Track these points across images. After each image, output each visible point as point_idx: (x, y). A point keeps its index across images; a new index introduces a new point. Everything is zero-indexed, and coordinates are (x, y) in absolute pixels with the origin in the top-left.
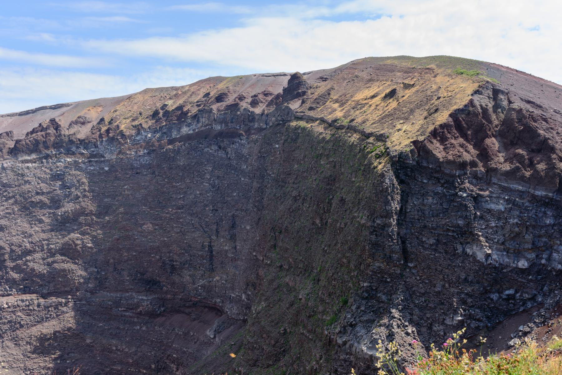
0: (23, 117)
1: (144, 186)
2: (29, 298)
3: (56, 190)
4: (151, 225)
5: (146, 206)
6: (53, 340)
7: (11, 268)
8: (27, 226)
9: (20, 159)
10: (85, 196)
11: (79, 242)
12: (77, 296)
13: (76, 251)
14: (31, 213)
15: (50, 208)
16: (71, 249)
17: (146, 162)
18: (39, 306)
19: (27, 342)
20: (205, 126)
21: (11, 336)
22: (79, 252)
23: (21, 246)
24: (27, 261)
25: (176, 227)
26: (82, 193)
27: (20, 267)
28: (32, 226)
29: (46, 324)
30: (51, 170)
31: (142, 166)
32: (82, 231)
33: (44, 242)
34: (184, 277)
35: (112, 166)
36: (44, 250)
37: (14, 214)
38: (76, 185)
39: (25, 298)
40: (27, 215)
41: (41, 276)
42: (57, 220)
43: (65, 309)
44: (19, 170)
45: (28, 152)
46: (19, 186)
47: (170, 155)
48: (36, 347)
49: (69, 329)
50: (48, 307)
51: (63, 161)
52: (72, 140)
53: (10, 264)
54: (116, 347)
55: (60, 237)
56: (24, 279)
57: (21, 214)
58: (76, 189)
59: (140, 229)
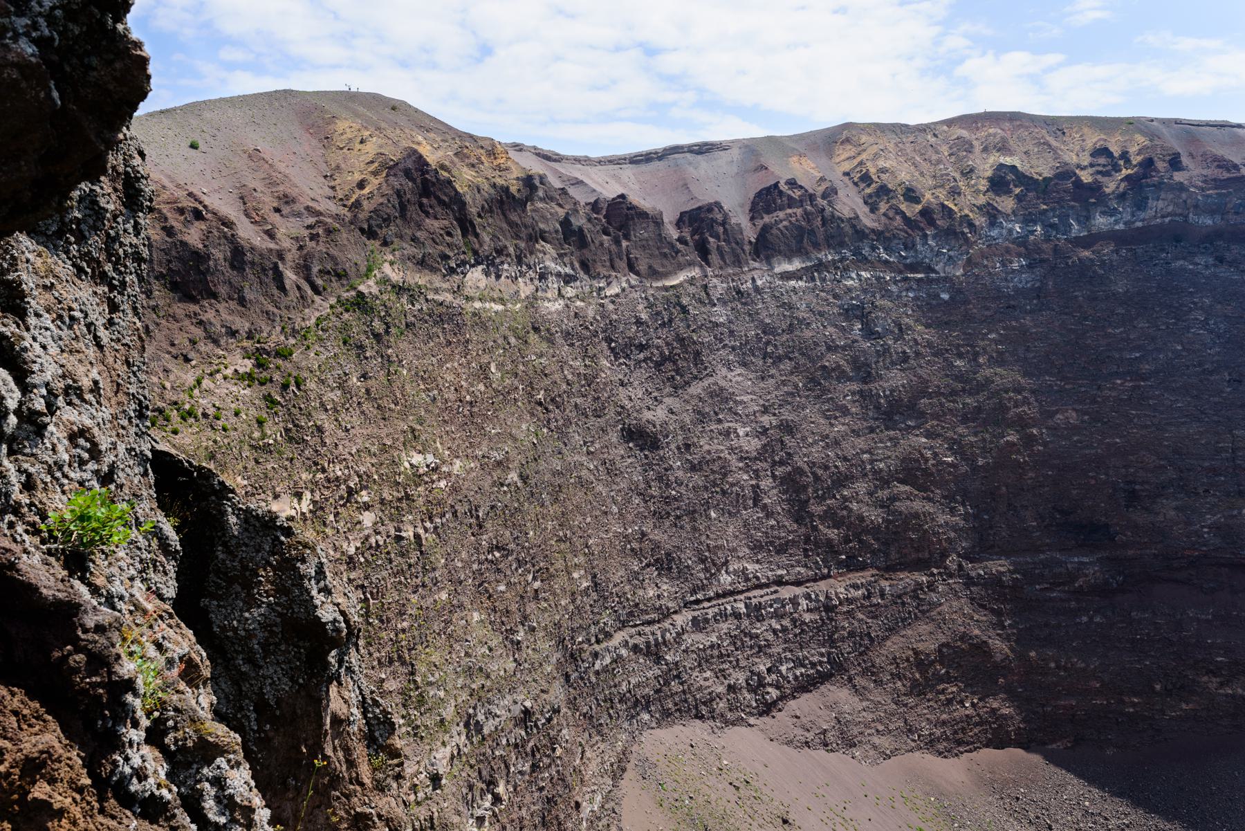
0: (644, 167)
1: (1036, 333)
2: (864, 581)
3: (856, 341)
4: (1074, 414)
5: (1051, 375)
6: (942, 664)
7: (820, 517)
8: (822, 421)
9: (778, 270)
10: (918, 354)
11: (929, 454)
12: (946, 568)
13: (926, 473)
14: (825, 391)
15: (850, 379)
16: (918, 469)
17: (1026, 283)
18: (882, 595)
19: (892, 674)
20: (1163, 217)
21: (859, 664)
22: (932, 474)
23: (826, 468)
24: (845, 499)
25: (1139, 416)
26: (911, 347)
27: (835, 513)
28: (833, 421)
29: (909, 632)
30: (836, 296)
31: (1019, 292)
32: (927, 430)
33: (866, 456)
34: (1157, 514)
35: (956, 291)
36: (866, 475)
37: (799, 396)
38: (892, 332)
39: (859, 582)
40: (819, 397)
41: (875, 531)
42: (878, 407)
43: (934, 597)
44: (782, 295)
45: (788, 253)
46: (791, 328)
47: (1095, 272)
48: (914, 681)
49: (963, 637)
50: (900, 597)
51: (854, 275)
52: (863, 231)
53: (816, 509)
54: (1056, 662)
55: (889, 444)
56: (847, 540)
57: (807, 397)
58: (896, 340)
59: (1050, 423)
